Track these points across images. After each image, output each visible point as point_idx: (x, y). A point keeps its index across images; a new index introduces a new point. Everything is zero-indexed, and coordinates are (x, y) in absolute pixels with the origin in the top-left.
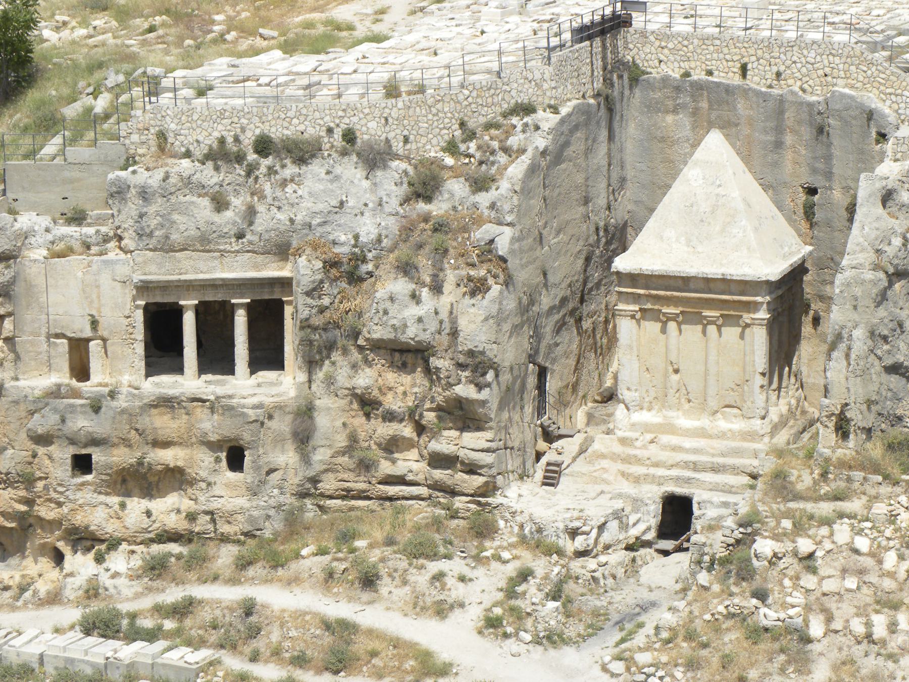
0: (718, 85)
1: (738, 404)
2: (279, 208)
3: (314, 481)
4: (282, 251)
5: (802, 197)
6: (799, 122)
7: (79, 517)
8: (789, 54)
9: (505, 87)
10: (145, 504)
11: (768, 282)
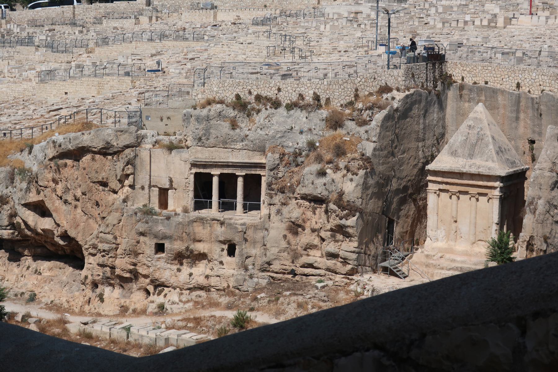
0: (490, 88)
2: (261, 129)
3: (269, 264)
4: (262, 150)
5: (527, 146)
6: (527, 108)
7: (157, 274)
8: (523, 75)
9: (379, 78)
10: (189, 270)
11: (499, 176)
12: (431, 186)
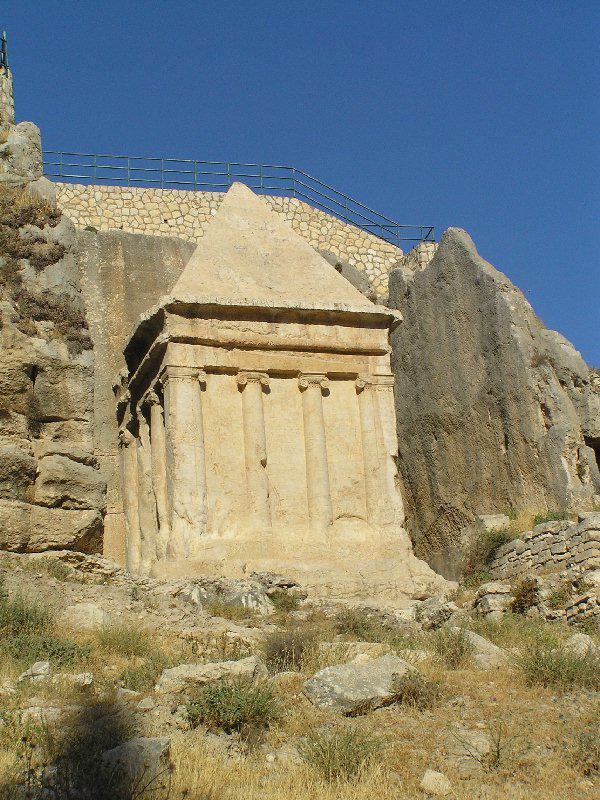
0: (137, 237)
1: (360, 510)
12: (178, 357)
